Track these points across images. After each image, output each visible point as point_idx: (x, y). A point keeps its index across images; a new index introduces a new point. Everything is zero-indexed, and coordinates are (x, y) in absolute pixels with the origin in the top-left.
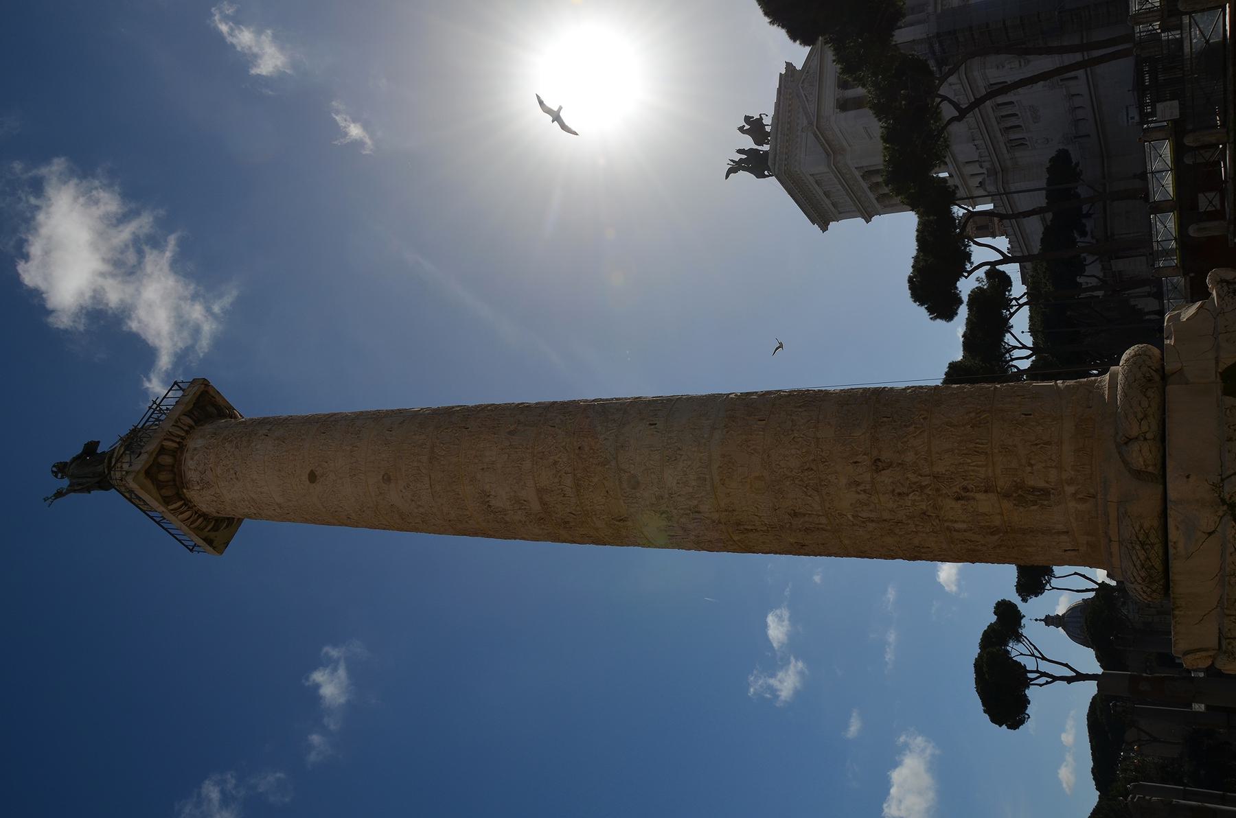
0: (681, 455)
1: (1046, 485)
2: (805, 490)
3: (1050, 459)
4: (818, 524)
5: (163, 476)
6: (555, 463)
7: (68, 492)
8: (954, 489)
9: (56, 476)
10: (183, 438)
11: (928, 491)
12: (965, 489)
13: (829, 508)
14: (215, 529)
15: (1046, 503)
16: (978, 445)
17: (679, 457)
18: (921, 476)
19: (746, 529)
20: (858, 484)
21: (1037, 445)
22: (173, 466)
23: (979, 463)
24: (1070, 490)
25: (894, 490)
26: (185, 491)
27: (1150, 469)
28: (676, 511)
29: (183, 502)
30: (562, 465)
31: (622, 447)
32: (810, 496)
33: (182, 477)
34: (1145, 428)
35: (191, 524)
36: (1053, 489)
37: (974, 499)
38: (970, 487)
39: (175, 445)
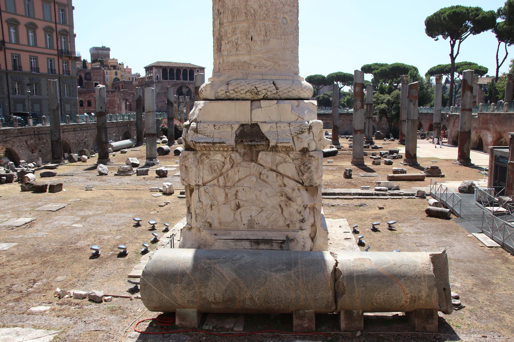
3: (230, 52)
34: (231, 92)
38: (221, 16)
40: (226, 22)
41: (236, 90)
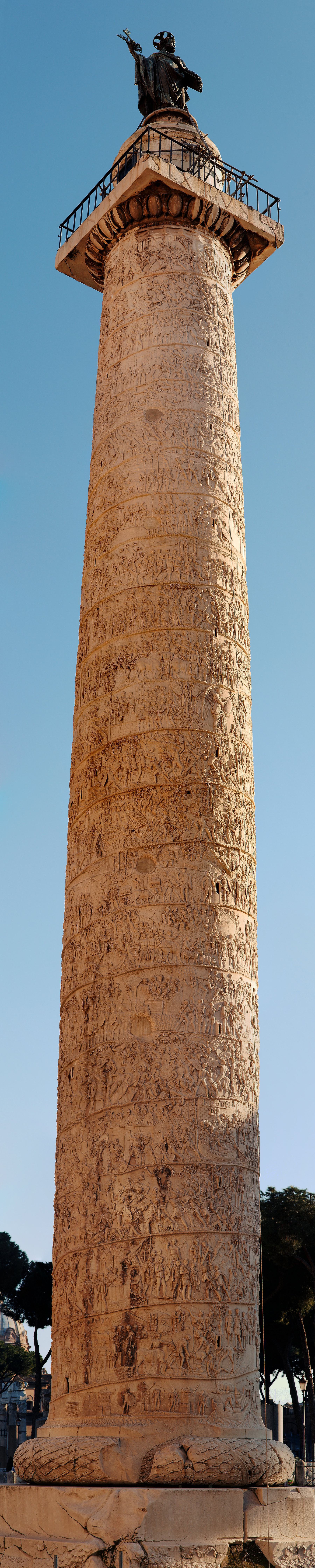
0: (178, 928)
1: (139, 1363)
2: (135, 1085)
3: (167, 1367)
4: (94, 1098)
5: (153, 201)
6: (170, 760)
7: (137, 58)
8: (134, 1261)
9: (156, 37)
10: (204, 224)
11: (132, 1229)
12: (135, 1273)
13: (113, 1113)
14: (89, 261)
15: (119, 1361)
16: (184, 1288)
17: (176, 925)
18: (150, 1223)
19: (88, 1008)
20: (141, 1148)
21: (184, 1352)
22: (168, 214)
23: (164, 1290)
24: (134, 1387)
25: (134, 1191)
26: (137, 229)
27: (154, 1472)
28: (110, 920)
29: (122, 227)
30: (167, 769)
31: (190, 850)
32: (127, 1090)
33: (154, 225)
35: (94, 235)
36: (134, 1369)
37: (124, 1283)
38: (137, 1278)
39: (195, 215)
40: (155, 1297)
41: (212, 1463)
